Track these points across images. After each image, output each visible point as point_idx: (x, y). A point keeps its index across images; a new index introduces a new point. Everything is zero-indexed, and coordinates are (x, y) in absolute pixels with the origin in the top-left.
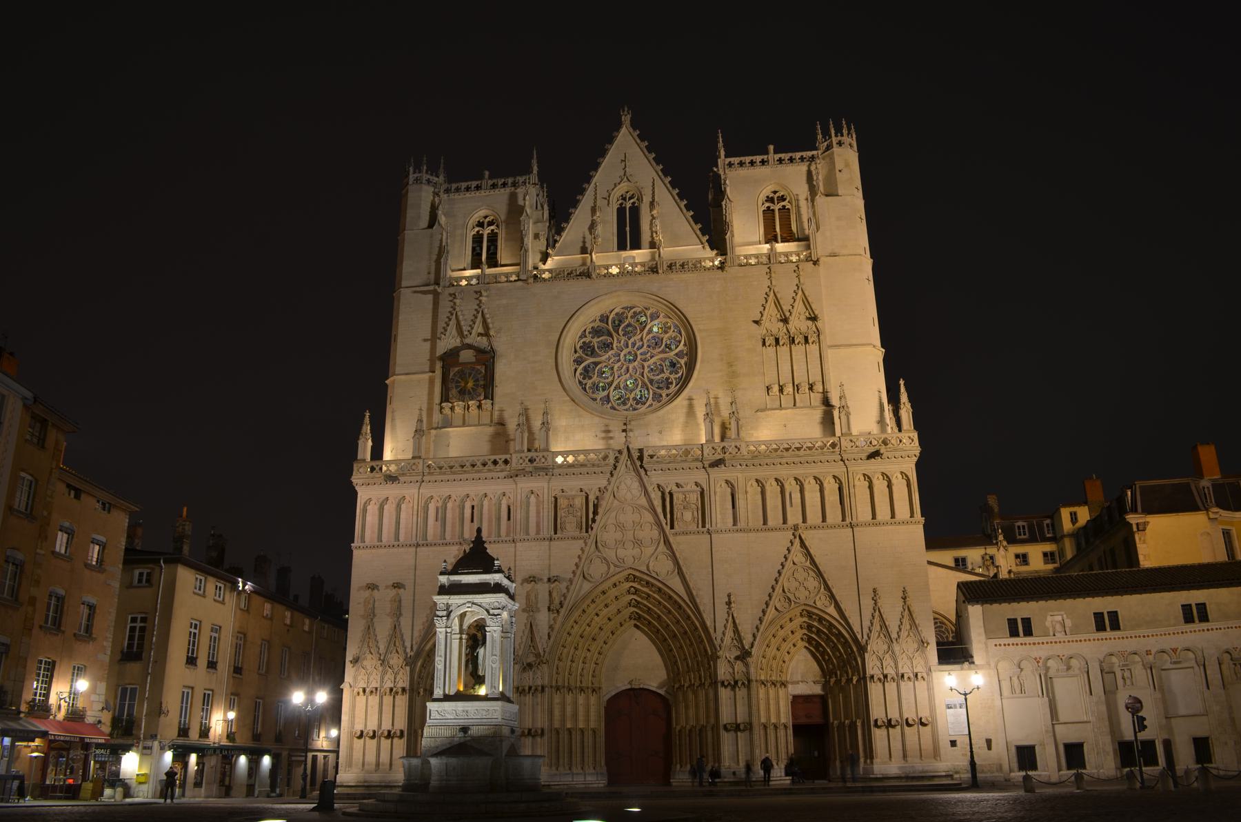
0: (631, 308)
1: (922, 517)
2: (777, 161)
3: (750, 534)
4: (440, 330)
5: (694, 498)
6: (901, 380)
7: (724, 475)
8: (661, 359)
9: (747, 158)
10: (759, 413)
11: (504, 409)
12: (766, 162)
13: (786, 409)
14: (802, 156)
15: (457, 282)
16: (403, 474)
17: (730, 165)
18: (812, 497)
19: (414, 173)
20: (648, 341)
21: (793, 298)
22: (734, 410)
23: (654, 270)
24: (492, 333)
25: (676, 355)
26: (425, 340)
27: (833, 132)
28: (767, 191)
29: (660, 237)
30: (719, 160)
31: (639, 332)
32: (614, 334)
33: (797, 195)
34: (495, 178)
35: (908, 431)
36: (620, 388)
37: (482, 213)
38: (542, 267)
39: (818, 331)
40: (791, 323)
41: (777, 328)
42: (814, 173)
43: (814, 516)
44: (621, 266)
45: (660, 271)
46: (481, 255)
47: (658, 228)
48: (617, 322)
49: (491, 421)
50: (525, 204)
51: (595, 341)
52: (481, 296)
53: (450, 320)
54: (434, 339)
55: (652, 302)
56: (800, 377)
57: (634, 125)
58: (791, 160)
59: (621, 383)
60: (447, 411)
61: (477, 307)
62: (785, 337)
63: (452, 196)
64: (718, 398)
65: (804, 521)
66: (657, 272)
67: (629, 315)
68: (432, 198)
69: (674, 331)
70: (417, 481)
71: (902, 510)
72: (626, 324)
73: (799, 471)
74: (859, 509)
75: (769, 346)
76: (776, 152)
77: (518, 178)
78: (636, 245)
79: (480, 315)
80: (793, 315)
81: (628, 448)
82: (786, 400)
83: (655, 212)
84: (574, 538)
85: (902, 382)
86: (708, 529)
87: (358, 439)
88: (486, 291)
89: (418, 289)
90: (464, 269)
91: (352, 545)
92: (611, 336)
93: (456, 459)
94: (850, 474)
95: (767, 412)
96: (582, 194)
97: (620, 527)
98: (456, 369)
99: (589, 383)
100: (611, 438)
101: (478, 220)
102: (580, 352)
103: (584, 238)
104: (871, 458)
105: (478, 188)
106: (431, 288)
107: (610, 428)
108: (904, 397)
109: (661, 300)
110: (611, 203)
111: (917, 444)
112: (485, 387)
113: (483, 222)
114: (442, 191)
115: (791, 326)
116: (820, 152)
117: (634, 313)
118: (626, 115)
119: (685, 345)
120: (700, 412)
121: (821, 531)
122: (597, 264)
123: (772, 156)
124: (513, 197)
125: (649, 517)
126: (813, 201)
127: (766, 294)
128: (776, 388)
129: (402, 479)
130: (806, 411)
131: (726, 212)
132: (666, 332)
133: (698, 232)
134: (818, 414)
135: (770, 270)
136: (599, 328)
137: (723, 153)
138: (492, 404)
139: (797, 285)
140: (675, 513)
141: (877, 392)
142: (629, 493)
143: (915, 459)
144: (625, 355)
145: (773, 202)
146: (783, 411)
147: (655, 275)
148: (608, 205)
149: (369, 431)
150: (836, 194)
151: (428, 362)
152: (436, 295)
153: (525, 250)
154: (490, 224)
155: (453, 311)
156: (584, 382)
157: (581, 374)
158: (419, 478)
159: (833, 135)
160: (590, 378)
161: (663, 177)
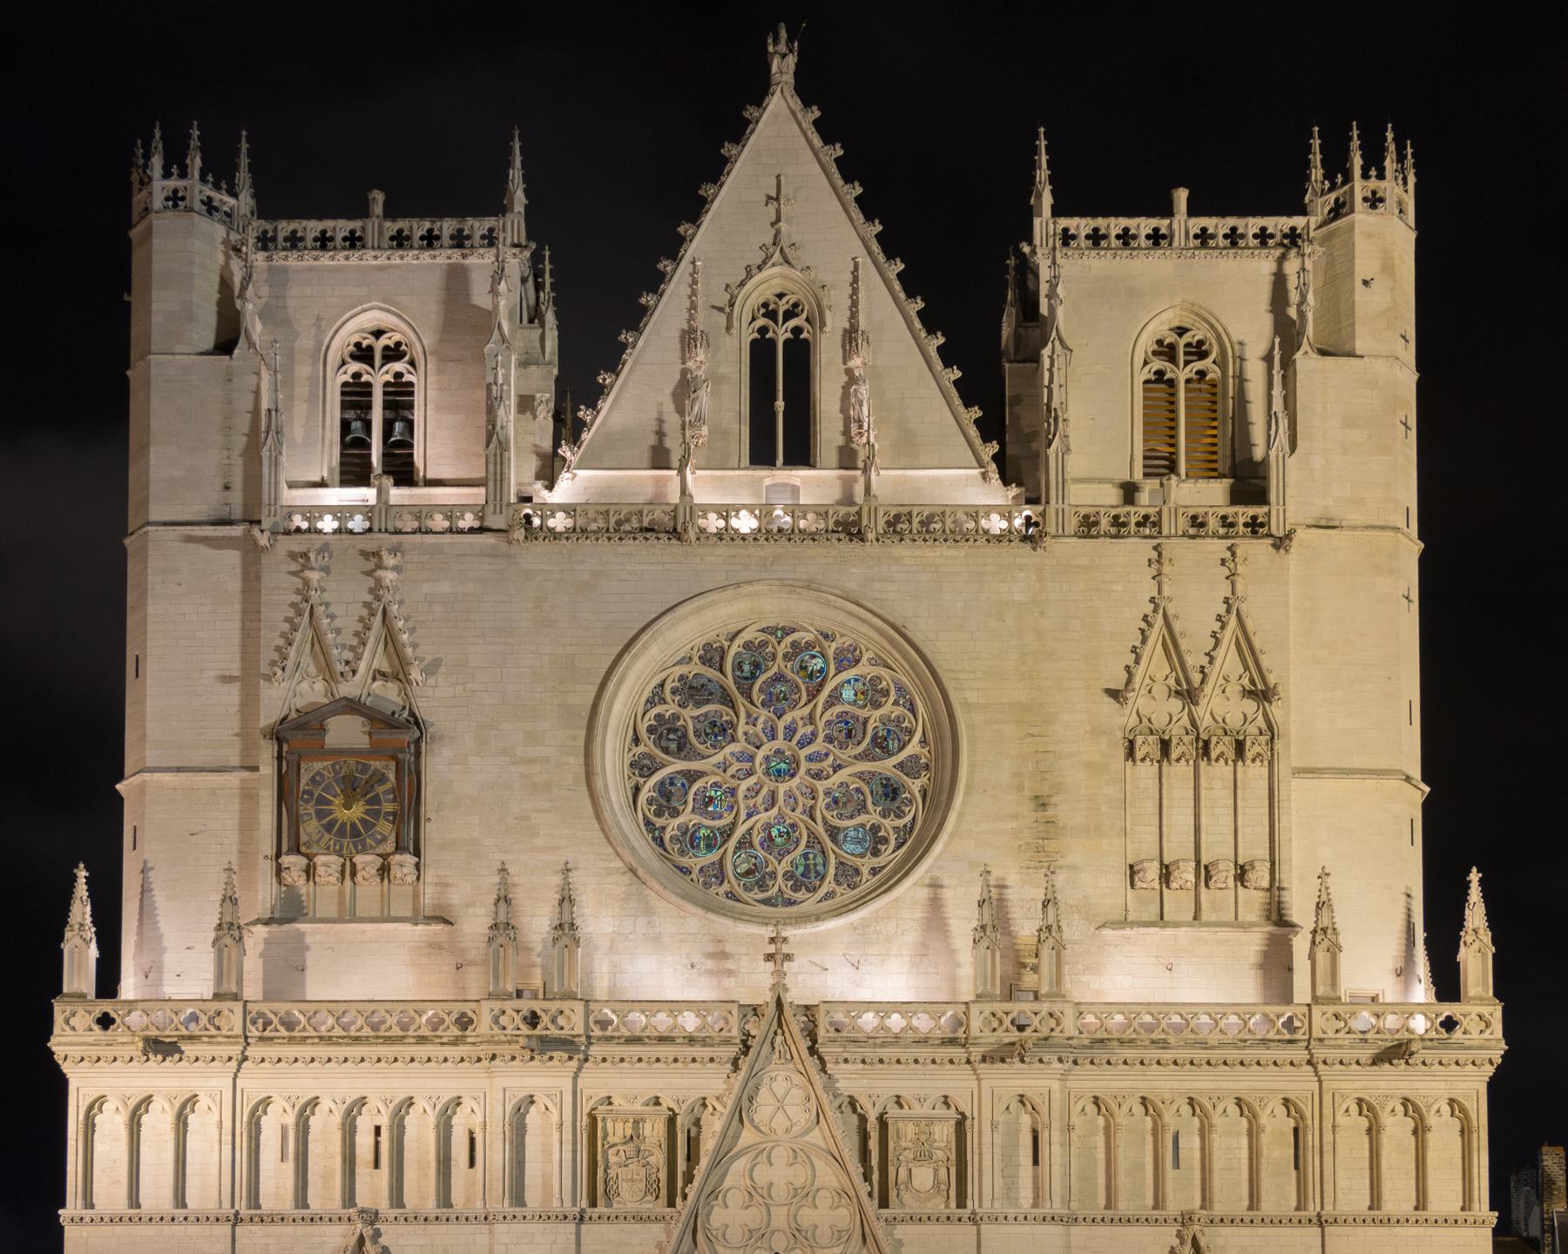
0: (787, 631)
1: (1492, 1208)
2: (1196, 236)
3: (1075, 1230)
4: (267, 654)
5: (944, 1133)
6: (1474, 870)
7: (1017, 1082)
8: (860, 776)
9: (1112, 220)
10: (1107, 932)
11: (450, 881)
12: (1164, 237)
13: (1177, 925)
14: (1263, 229)
15: (308, 519)
16: (191, 1038)
17: (1067, 237)
18: (1230, 1147)
19: (167, 175)
20: (829, 723)
21: (1214, 635)
22: (1051, 920)
23: (851, 529)
24: (415, 674)
25: (901, 766)
26: (226, 679)
27: (1357, 162)
28: (1160, 327)
29: (874, 436)
30: (1037, 222)
31: (804, 698)
32: (740, 700)
33: (1241, 344)
34: (405, 216)
35: (1481, 1000)
36: (751, 846)
37: (372, 318)
38: (543, 495)
39: (1271, 728)
40: (1203, 702)
41: (1164, 710)
42: (1292, 283)
43: (1230, 1194)
44: (765, 512)
45: (871, 536)
46: (364, 444)
47: (865, 409)
48: (746, 668)
49: (416, 910)
50: (496, 306)
51: (689, 715)
52: (380, 566)
53: (295, 629)
54: (249, 678)
55: (841, 617)
56: (1217, 848)
57: (806, 90)
58: (1233, 237)
59: (755, 832)
60: (295, 876)
61: (369, 598)
62: (1186, 739)
63: (279, 258)
64: (1005, 887)
65: (1206, 1202)
66: (860, 535)
67: (781, 650)
68: (221, 259)
69: (896, 703)
70: (230, 1059)
71: (1445, 1194)
72: (770, 673)
73: (1201, 1083)
74: (1341, 1184)
75: (1143, 760)
76: (1193, 211)
77: (470, 221)
78: (800, 455)
79: (377, 621)
80: (1211, 681)
81: (779, 1004)
82: (1178, 902)
83: (856, 362)
84: (639, 1218)
85: (1474, 876)
86: (974, 1213)
87: (61, 938)
88: (394, 551)
89: (197, 531)
90: (322, 484)
91: (60, 1212)
92: (732, 704)
93: (361, 1006)
94: (1327, 1099)
95: (1128, 932)
96: (655, 292)
97: (756, 1194)
98: (318, 766)
99: (672, 826)
100: (730, 973)
101: (356, 338)
102: (648, 746)
103: (661, 421)
104: (1382, 1061)
105: (354, 241)
106: (237, 531)
107: (729, 948)
108: (1476, 915)
109: (869, 616)
110: (736, 323)
111: (1499, 1033)
112: (397, 818)
113: (370, 348)
114: (251, 241)
115: (1201, 711)
116: (1314, 221)
117: (794, 644)
118: (784, 56)
119: (924, 742)
120: (962, 919)
121: (1245, 1231)
122: (697, 500)
123: (1182, 223)
124: (457, 279)
125: (828, 1175)
126: (1288, 364)
127: (1145, 619)
128: (1152, 872)
129: (189, 1049)
130: (1223, 934)
131: (1051, 381)
132: (877, 705)
133: (973, 432)
134: (1253, 943)
135: (1160, 555)
136: (702, 681)
137: (1047, 200)
138: (417, 866)
139: (1226, 600)
140: (892, 1170)
141: (1404, 897)
142: (780, 1113)
143: (1490, 1070)
144: (767, 758)
145: (1172, 359)
146: (1169, 932)
147: (856, 544)
148: (728, 328)
149: (89, 920)
150: (1347, 348)
151: (237, 740)
152: (252, 554)
153: (500, 443)
154: (394, 353)
155: (305, 607)
156: (659, 822)
157: (650, 802)
158: (236, 1050)
159: (1357, 172)
160: (675, 813)
161: (881, 258)
